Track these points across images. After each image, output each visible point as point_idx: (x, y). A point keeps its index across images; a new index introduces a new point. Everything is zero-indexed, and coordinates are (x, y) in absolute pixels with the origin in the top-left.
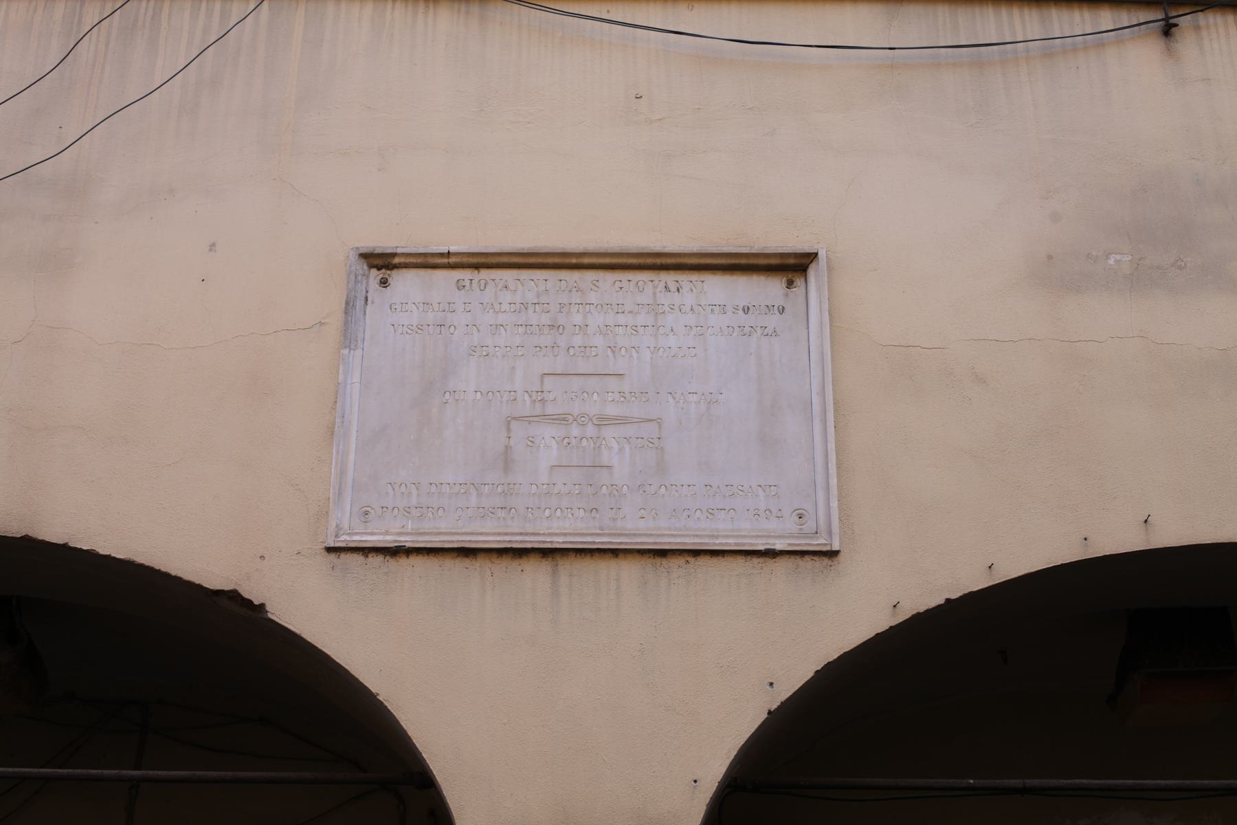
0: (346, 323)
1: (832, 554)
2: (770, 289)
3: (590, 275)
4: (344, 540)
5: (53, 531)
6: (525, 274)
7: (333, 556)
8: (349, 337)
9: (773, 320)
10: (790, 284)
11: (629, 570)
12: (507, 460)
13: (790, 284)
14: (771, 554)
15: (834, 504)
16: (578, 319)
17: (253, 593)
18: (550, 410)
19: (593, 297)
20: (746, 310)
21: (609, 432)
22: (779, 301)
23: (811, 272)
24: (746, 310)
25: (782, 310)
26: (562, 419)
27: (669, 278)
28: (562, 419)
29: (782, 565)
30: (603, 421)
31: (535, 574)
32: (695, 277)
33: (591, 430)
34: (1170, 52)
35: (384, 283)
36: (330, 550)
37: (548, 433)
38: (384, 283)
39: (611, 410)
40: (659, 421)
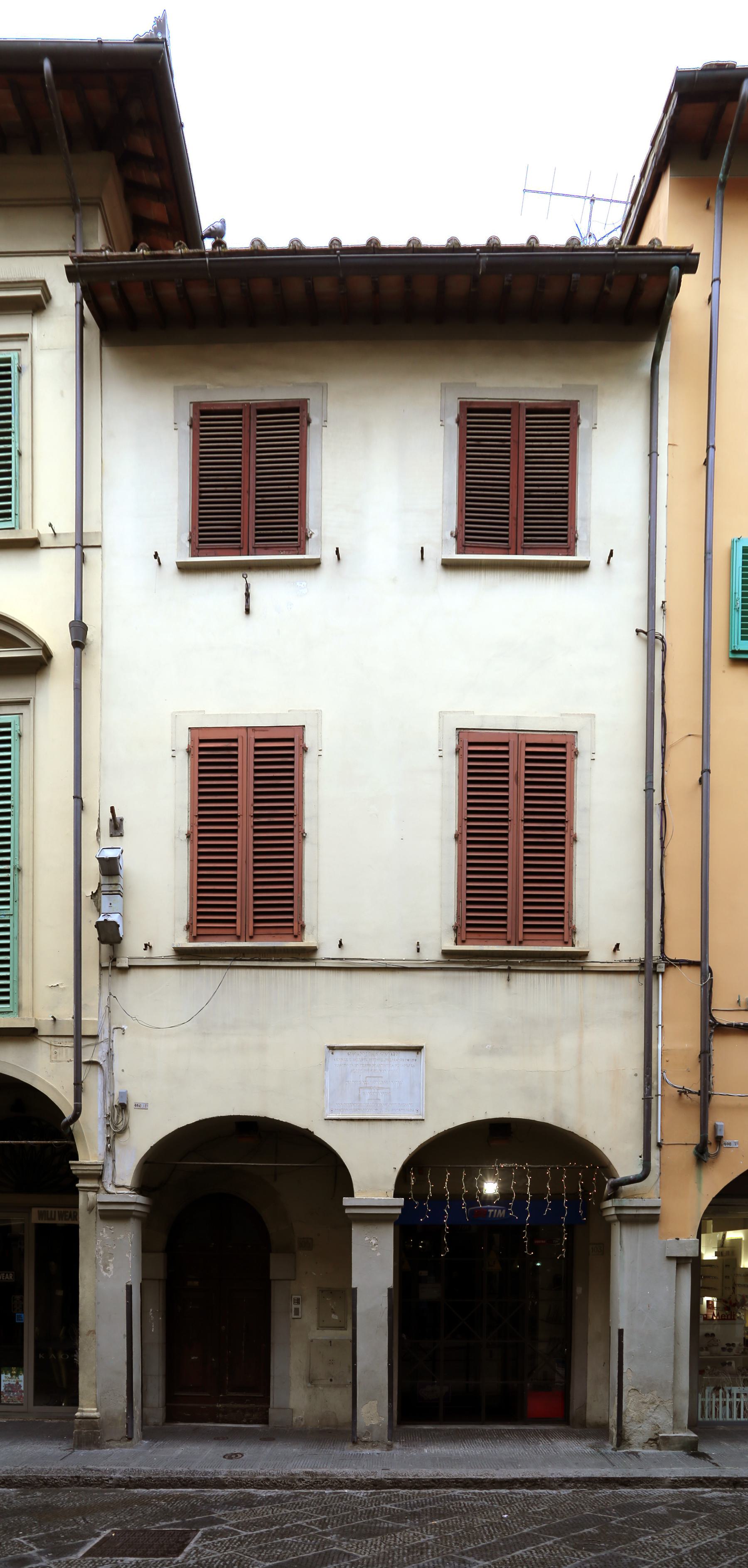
0: (326, 1064)
1: (423, 1120)
2: (412, 1055)
3: (375, 1052)
4: (328, 1117)
5: (271, 1115)
6: (362, 1051)
7: (326, 1121)
8: (326, 1068)
9: (414, 1063)
10: (418, 1054)
11: (383, 1124)
12: (359, 1098)
13: (418, 1054)
14: (411, 1120)
15: (424, 1109)
16: (373, 1063)
17: (311, 1129)
18: (368, 1086)
19: (376, 1057)
20: (408, 1060)
21: (380, 1091)
22: (415, 1058)
23: (422, 1050)
24: (408, 1060)
25: (416, 1060)
26: (370, 1088)
27: (392, 1052)
28: (370, 1088)
29: (412, 1122)
30: (379, 1088)
31: (365, 1125)
32: (398, 1052)
33: (376, 1091)
34: (509, 986)
35: (332, 1053)
36: (325, 1119)
37: (367, 1091)
38: (332, 1053)
39: (380, 1086)
40: (389, 1088)
